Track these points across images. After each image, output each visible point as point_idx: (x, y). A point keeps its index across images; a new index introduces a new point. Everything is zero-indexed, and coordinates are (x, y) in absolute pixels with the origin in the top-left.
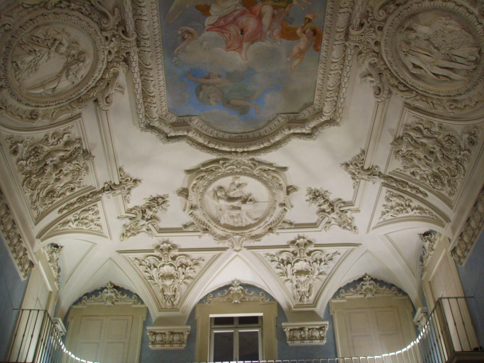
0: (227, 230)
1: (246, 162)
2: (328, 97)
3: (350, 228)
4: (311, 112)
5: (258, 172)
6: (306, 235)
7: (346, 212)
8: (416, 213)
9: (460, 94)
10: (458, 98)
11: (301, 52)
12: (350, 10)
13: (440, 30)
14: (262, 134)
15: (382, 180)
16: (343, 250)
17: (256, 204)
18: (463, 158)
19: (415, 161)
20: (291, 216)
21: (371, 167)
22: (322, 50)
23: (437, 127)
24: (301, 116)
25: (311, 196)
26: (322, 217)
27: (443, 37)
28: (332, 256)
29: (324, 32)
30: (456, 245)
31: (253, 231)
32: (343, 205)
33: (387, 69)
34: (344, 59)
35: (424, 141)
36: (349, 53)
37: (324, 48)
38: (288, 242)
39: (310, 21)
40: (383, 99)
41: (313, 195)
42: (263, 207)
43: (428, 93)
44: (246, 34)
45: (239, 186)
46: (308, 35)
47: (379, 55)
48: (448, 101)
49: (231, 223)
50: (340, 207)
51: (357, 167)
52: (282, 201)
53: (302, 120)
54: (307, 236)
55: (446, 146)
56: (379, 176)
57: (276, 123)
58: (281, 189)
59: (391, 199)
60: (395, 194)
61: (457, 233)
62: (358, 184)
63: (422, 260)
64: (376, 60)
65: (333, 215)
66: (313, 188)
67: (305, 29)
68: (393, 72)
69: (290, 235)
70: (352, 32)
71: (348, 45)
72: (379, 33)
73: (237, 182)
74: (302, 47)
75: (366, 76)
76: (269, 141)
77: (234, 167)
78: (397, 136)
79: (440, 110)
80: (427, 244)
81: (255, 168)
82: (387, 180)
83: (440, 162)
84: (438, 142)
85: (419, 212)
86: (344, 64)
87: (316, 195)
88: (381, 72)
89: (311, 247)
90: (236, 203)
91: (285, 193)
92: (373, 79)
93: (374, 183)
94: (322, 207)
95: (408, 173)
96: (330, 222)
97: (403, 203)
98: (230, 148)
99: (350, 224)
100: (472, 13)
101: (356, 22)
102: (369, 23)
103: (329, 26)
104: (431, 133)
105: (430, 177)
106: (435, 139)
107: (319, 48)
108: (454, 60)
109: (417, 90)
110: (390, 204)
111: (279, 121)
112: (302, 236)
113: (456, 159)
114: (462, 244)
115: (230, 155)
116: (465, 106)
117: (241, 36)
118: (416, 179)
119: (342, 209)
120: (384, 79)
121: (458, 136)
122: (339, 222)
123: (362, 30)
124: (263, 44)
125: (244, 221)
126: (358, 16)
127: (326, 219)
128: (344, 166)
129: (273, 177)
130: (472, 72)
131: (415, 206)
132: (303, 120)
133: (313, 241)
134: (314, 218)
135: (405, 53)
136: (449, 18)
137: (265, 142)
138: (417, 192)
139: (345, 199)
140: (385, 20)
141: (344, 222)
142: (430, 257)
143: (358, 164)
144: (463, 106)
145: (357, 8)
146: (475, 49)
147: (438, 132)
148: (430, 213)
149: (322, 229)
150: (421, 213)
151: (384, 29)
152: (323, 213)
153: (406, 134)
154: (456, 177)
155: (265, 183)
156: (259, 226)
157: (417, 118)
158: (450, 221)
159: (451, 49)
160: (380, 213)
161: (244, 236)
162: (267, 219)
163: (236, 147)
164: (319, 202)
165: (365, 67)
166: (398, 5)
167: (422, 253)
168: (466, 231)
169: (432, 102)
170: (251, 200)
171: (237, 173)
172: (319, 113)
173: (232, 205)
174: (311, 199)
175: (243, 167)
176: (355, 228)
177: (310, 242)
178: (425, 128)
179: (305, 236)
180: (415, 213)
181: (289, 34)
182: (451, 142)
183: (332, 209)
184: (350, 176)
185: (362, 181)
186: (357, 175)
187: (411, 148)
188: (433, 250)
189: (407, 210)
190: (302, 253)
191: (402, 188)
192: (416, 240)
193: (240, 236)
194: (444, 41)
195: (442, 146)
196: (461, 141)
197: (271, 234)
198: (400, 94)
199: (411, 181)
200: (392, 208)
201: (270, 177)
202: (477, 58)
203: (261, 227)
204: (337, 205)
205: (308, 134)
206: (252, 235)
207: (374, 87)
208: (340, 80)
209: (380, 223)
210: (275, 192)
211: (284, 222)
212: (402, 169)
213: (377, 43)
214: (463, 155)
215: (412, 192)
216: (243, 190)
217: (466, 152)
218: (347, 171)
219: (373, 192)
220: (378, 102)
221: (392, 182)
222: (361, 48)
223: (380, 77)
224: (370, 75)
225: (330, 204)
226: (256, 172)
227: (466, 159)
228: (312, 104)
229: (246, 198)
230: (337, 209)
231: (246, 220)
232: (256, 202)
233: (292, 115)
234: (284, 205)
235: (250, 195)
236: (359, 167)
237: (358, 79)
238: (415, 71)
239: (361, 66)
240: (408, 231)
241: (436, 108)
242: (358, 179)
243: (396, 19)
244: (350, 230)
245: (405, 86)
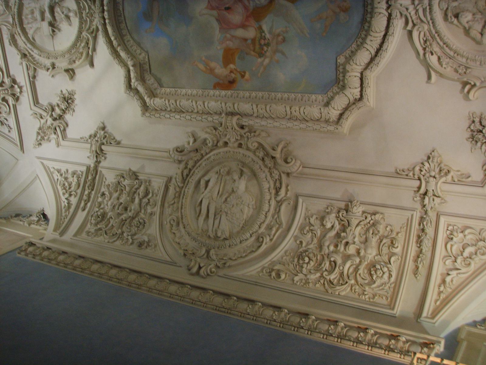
0: (16, 7)
1: (94, 23)
2: (169, 101)
3: (38, 139)
4: (153, 86)
5: (85, 36)
6: (25, 94)
7: (55, 133)
8: (64, 203)
9: (184, 228)
10: (181, 226)
11: (211, 71)
12: (255, 115)
13: (243, 201)
14: (125, 38)
15: (92, 165)
16: (14, 134)
17: (51, 37)
18: (125, 238)
19: (116, 195)
20: (43, 76)
21: (104, 152)
22: (215, 91)
23: (152, 210)
24: (147, 76)
25: (67, 95)
26: (46, 109)
27: (237, 204)
28: (6, 124)
29: (232, 92)
30: (38, 245)
31: (20, 37)
32: (62, 129)
33: (202, 156)
34: (209, 113)
35: (137, 201)
36: (214, 118)
37: (217, 92)
38: (13, 75)
39: (243, 76)
40: (173, 156)
41: (68, 97)
42: (48, 45)
43: (183, 197)
44: (225, 13)
45: (68, 17)
46: (229, 76)
47: (215, 147)
48: (177, 218)
49: (26, 11)
50: (59, 126)
51: (102, 139)
52: (57, 65)
53: (144, 77)
54: (23, 96)
55: (134, 221)
56: (96, 162)
57: (138, 51)
58: (70, 63)
59: (75, 176)
60: (80, 180)
61: (50, 245)
62: (86, 142)
63: (17, 215)
64: (210, 145)
65: (50, 121)
66: (76, 96)
67: (235, 72)
68: (200, 162)
69: (22, 78)
70: (235, 119)
71: (222, 116)
72: (236, 145)
73: (71, 14)
74: (217, 71)
75: (193, 136)
76: (119, 45)
77: (87, 11)
78: (138, 174)
79: (168, 211)
80: (35, 218)
81: (89, 34)
82: (94, 170)
83: (118, 218)
84: (137, 214)
85: (65, 205)
86: (203, 115)
87: (68, 100)
88: (198, 150)
89: (12, 101)
90: (48, 15)
91: (66, 68)
92: (191, 144)
93: (88, 157)
94: (57, 108)
95: (103, 190)
96: (42, 118)
97: (72, 189)
98: (107, 4)
99: (43, 138)
100: (260, 227)
101: (245, 121)
103: (239, 96)
104: (145, 206)
105: (102, 211)
106: (139, 210)
107: (217, 88)
108: (216, 217)
109: (184, 187)
110: (69, 176)
111: (140, 54)
112: (23, 91)
113: (123, 233)
114: (40, 251)
115: (99, 5)
116: (174, 233)
117: (223, 8)
118: (98, 197)
119: (58, 129)
120: (192, 154)
121: (146, 231)
122: (43, 127)
123: (237, 128)
124: (217, 31)
125: (30, 26)
126: (251, 123)
127: (44, 114)
128: (102, 125)
129: (82, 54)
130: (206, 235)
131: (71, 201)
132: (144, 79)
133: (18, 103)
134: (44, 101)
135: (219, 172)
136: (255, 207)
137: (117, 41)
138: (86, 201)
139: (68, 131)
140: (248, 149)
141: (44, 133)
142: (21, 223)
143: (105, 139)
145: (258, 121)
146: (227, 235)
147: (147, 212)
148: (66, 216)
149: (33, 110)
150: (64, 207)
151: (240, 149)
152: (50, 109)
153: (141, 183)
154: (105, 235)
155: (74, 45)
156: (26, 42)
157: (158, 191)
158: (61, 236)
159: (226, 213)
160: (59, 168)
161: (13, 27)
162: (35, 51)
163: (108, 11)
164: (61, 104)
165: (202, 135)
166: (263, 159)
167: (24, 215)
168: (53, 252)
169: (174, 203)
170: (53, 31)
171: (81, 13)
172: (153, 95)
173: (45, 11)
174: (64, 95)
175: (88, 20)
176: (40, 144)
177: (17, 99)
178: (149, 200)
179: (23, 93)
180: (64, 202)
181: (228, 57)
182: (138, 226)
183: (56, 118)
184: (93, 132)
185: (89, 145)
186: (94, 140)
187: (128, 189)
188: (29, 225)
189: (66, 194)
190: (4, 92)
191: (87, 185)
192: (37, 207)
193: (12, 23)
194: (233, 206)
195: (133, 218)
196: (140, 235)
197: (19, 57)
198: (179, 172)
199: (96, 193)
200: (66, 179)
201: (81, 50)
203: (26, 45)
204: (61, 123)
205: (130, 85)
206: (16, 35)
207: (184, 146)
208: (188, 111)
209: (49, 169)
210: (66, 57)
211: (35, 70)
212: (107, 183)
213: (226, 144)
214: (127, 239)
215: (84, 196)
216: (64, 23)
217: (131, 240)
218: (97, 129)
219: (79, 157)
220: (170, 151)
221: (92, 175)
222: (220, 129)
223: (194, 151)
224: (195, 141)
225: (61, 116)
226: (84, 34)
227: (124, 242)
228: (161, 86)
229: (55, 26)
230: (56, 123)
231: (31, 28)
232: (53, 37)
233: (147, 67)
234: (54, 68)
235: (59, 30)
236: (102, 141)
237: (190, 130)
238: (203, 183)
239: (203, 130)
240: (44, 198)
241: (169, 207)
242: (91, 142)
243: (250, 159)
244: (37, 139)
245: (187, 175)
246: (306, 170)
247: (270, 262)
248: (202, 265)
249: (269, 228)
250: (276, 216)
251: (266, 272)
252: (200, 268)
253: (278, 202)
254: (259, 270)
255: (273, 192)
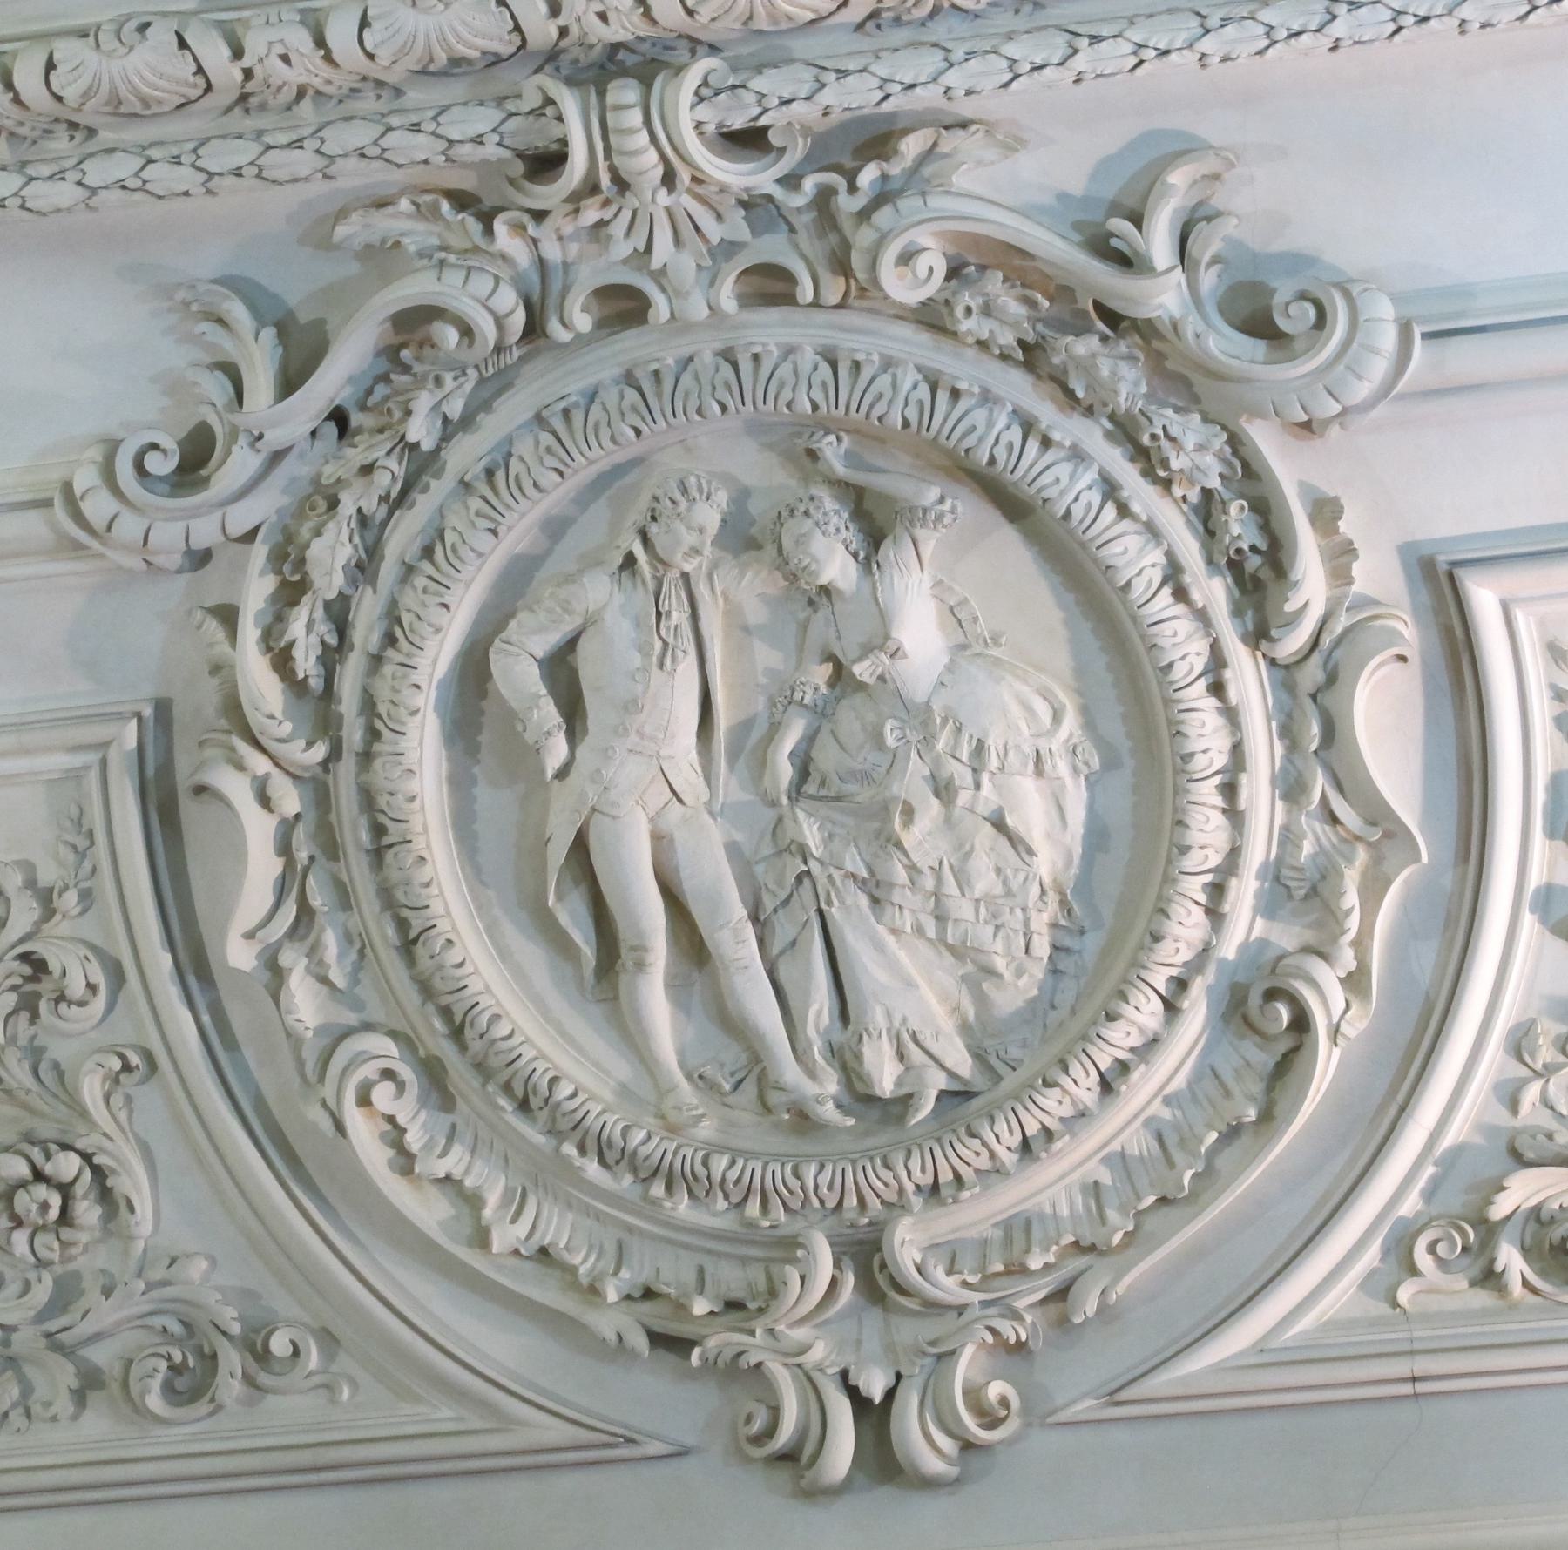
88: (356, 419)
102: (791, 181)
144: (441, 1168)
151: (774, 314)
166: (1031, 356)
202: (905, 1102)
213: (623, 307)
243: (909, 377)
245: (331, 658)
246: (1465, 359)
247: (1430, 1170)
248: (875, 1385)
249: (1302, 892)
250: (1319, 783)
251: (1442, 1263)
252: (873, 1416)
253: (1284, 673)
254: (1371, 1256)
255: (1214, 591)
